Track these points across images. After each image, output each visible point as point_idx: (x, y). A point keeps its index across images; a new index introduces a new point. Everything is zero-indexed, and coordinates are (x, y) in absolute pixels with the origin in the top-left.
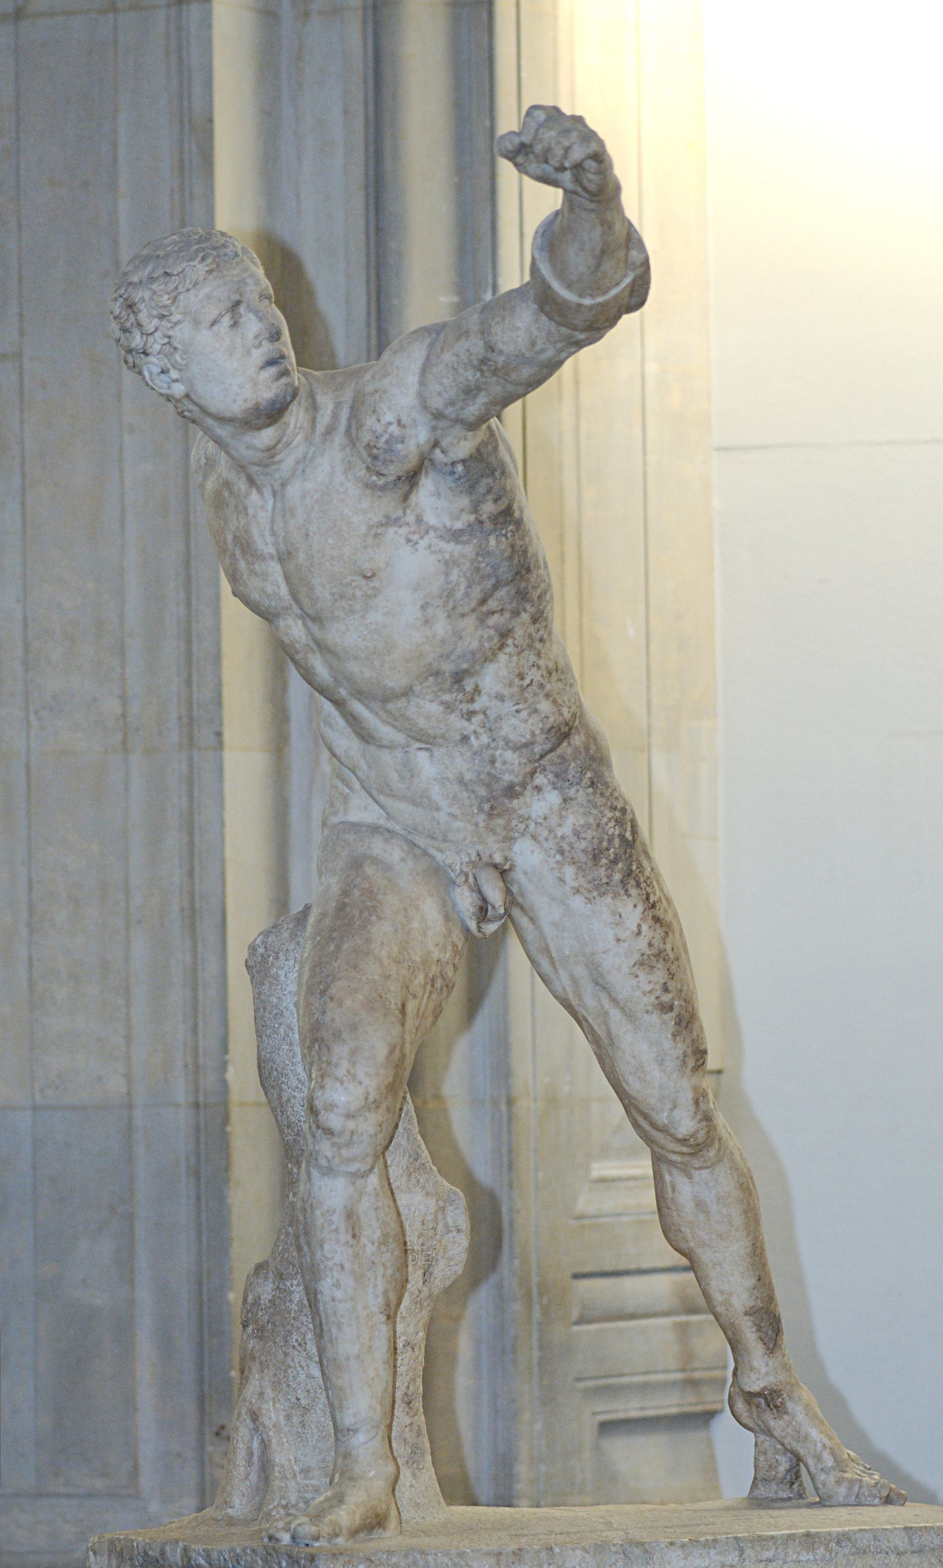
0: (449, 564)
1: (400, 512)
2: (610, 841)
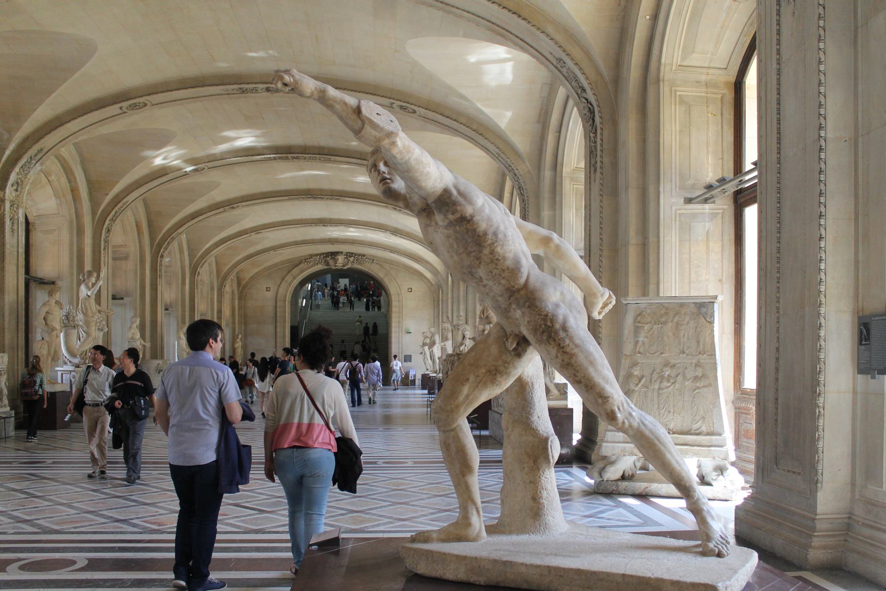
0: (448, 237)
1: (428, 222)
2: (540, 326)
